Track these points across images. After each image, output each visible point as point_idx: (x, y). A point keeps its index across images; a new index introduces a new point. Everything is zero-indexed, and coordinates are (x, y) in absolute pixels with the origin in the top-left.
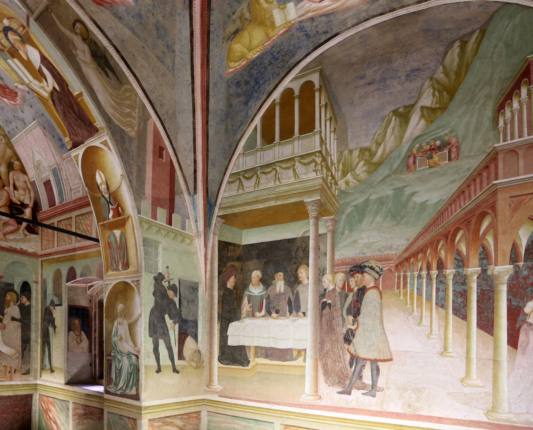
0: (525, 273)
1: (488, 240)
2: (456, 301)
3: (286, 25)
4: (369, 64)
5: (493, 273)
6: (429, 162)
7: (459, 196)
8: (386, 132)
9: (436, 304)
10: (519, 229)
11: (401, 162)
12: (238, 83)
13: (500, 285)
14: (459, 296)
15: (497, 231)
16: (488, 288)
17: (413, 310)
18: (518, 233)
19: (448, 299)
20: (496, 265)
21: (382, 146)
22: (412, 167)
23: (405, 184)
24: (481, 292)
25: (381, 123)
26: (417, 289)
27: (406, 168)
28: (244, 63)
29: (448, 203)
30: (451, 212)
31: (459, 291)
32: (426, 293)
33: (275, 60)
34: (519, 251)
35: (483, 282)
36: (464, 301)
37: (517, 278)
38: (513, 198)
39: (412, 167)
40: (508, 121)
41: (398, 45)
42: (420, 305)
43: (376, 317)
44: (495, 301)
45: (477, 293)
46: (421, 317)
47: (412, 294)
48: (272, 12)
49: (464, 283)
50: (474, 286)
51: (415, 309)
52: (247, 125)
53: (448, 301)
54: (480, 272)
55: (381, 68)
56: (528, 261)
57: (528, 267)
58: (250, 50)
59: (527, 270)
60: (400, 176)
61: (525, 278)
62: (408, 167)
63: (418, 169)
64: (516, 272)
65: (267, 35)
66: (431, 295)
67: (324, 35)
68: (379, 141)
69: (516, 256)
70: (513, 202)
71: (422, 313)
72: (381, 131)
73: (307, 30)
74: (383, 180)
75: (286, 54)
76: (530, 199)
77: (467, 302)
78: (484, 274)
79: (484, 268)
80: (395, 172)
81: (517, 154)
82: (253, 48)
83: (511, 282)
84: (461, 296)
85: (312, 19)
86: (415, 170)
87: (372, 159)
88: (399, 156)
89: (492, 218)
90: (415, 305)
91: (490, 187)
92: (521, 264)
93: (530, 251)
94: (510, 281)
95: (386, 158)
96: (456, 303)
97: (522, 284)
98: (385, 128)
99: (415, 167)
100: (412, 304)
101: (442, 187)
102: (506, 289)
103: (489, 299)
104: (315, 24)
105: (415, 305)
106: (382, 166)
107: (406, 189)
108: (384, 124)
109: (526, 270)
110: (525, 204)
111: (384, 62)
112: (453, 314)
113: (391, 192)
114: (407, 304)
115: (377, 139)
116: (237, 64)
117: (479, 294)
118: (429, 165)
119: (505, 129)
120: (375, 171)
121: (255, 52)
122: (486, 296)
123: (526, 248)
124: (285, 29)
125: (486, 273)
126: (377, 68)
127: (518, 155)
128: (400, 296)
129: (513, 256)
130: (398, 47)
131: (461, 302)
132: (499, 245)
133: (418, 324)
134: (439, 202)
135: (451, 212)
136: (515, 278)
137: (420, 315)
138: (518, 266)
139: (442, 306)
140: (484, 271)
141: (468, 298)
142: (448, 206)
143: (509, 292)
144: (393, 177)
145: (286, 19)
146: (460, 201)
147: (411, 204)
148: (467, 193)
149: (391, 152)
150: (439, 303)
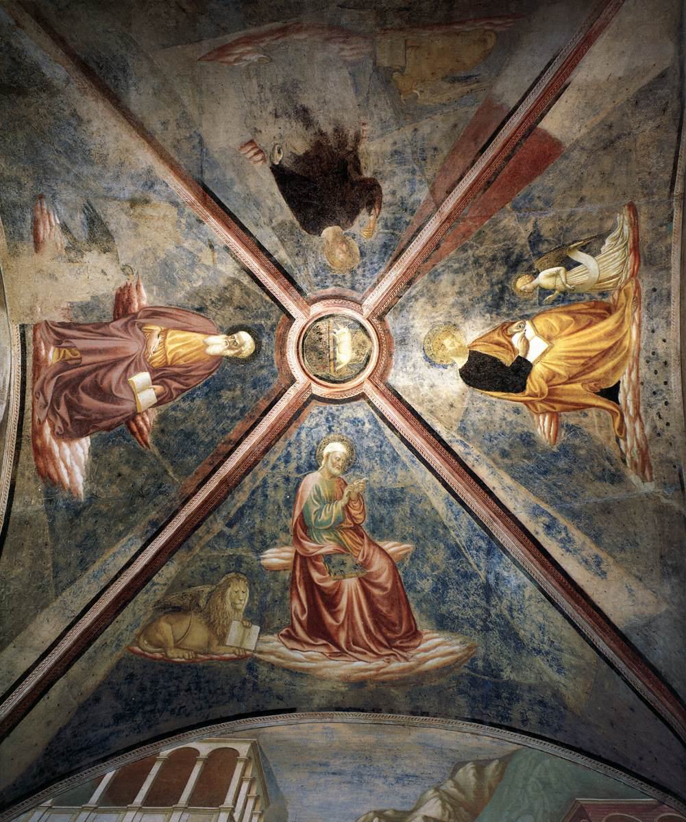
3: (237, 650)
12: (132, 675)
28: (158, 655)
33: (196, 689)
48: (231, 621)
52: (92, 760)
58: (177, 647)
65: (209, 644)
67: (277, 701)
73: (260, 677)
75: (215, 692)
82: (182, 646)
85: (272, 666)
104: (272, 675)
116: (151, 649)
121: (181, 655)
124: (233, 655)
145: (242, 642)
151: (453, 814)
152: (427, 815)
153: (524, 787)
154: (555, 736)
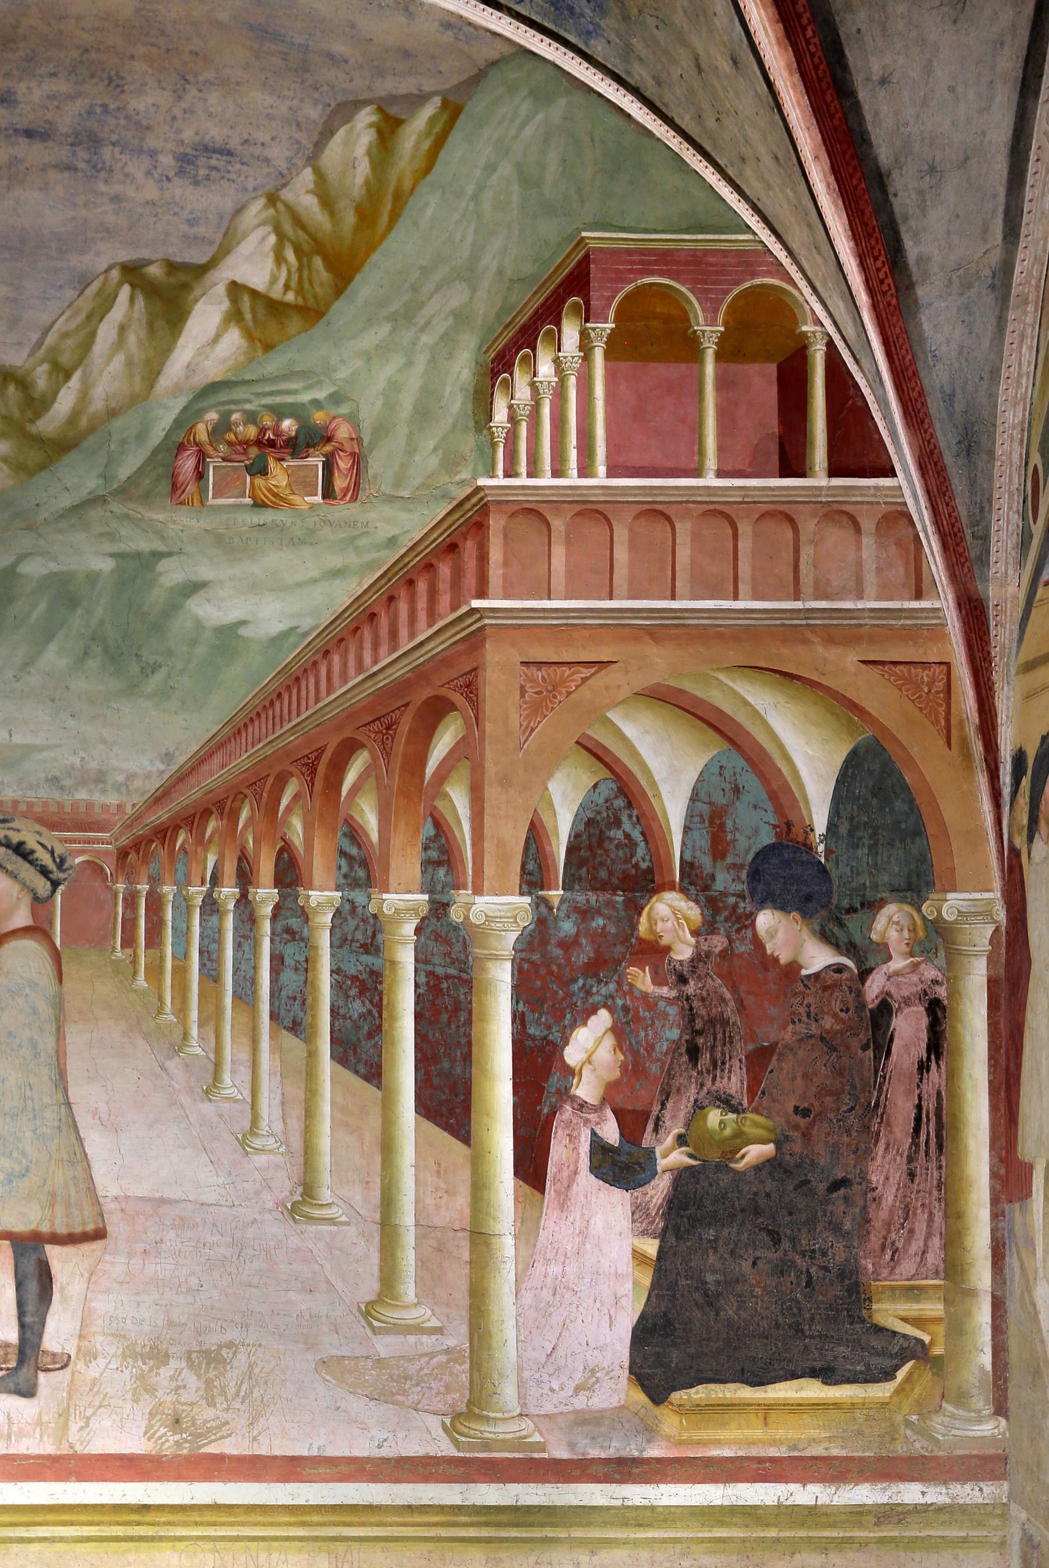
0: (568, 927)
1: (451, 801)
2: (342, 1011)
4: (29, 59)
5: (467, 917)
6: (252, 483)
7: (357, 629)
8: (93, 334)
9: (274, 1016)
10: (550, 775)
11: (149, 461)
13: (490, 965)
14: (353, 992)
15: (483, 773)
16: (452, 971)
17: (186, 1036)
18: (547, 789)
19: (316, 1000)
20: (478, 890)
21: (75, 382)
22: (191, 488)
23: (163, 548)
24: (428, 983)
25: (70, 294)
26: (201, 952)
27: (165, 487)
29: (319, 644)
30: (329, 679)
31: (353, 972)
32: (236, 970)
34: (548, 848)
35: (437, 948)
36: (370, 1012)
37: (544, 942)
38: (533, 669)
39: (191, 488)
40: (523, 413)
41: (153, 40)
42: (211, 1017)
43: (37, 1055)
44: (474, 1018)
45: (417, 986)
46: (218, 1066)
47: (181, 971)
49: (372, 946)
50: (406, 958)
51: (194, 1032)
53: (314, 1007)
54: (424, 910)
55: (79, 95)
56: (577, 887)
57: (577, 909)
59: (574, 917)
60: (143, 511)
61: (568, 945)
62: (174, 487)
63: (211, 501)
64: (541, 922)
66: (254, 982)
68: (65, 359)
69: (540, 866)
70: (531, 680)
71: (218, 1049)
72: (74, 324)
74: (77, 509)
76: (584, 680)
77: (381, 1016)
78: (438, 919)
79: (437, 896)
80: (124, 492)
81: (548, 524)
83: (524, 955)
84: (362, 993)
86: (202, 503)
87: (32, 421)
88: (141, 437)
89: (468, 725)
90: (194, 1014)
91: (461, 619)
92: (555, 894)
93: (582, 853)
94: (521, 951)
95: (91, 430)
96: (344, 1017)
97: (559, 966)
98: (89, 317)
99: (203, 492)
100: (182, 1010)
101: (299, 585)
102: (508, 978)
103: (457, 1009)
105: (194, 1014)
106: (71, 457)
107: (164, 565)
108: (86, 302)
109: (568, 917)
110: (569, 693)
111: (92, 76)
112: (332, 1057)
113: (106, 565)
114: (160, 1010)
115: (54, 350)
117: (421, 991)
118: (253, 496)
119: (512, 437)
120: (42, 467)
122: (447, 999)
123: (569, 841)
125: (446, 915)
126: (61, 86)
127: (550, 530)
128: (135, 973)
129: (531, 866)
130: (152, 45)
131: (362, 1016)
132: (488, 820)
133: (207, 1092)
134: (285, 635)
135: (329, 679)
136: (536, 942)
137: (212, 1056)
138: (545, 901)
139: (295, 1027)
140: (439, 908)
141: (385, 1002)
142: (318, 657)
143: (520, 989)
144: (116, 507)
146: (361, 648)
147: (180, 625)
148: (384, 622)
149: (112, 413)
150: (283, 1013)
151: (295, 277)
152: (239, 280)
153: (475, 198)
154: (586, 44)
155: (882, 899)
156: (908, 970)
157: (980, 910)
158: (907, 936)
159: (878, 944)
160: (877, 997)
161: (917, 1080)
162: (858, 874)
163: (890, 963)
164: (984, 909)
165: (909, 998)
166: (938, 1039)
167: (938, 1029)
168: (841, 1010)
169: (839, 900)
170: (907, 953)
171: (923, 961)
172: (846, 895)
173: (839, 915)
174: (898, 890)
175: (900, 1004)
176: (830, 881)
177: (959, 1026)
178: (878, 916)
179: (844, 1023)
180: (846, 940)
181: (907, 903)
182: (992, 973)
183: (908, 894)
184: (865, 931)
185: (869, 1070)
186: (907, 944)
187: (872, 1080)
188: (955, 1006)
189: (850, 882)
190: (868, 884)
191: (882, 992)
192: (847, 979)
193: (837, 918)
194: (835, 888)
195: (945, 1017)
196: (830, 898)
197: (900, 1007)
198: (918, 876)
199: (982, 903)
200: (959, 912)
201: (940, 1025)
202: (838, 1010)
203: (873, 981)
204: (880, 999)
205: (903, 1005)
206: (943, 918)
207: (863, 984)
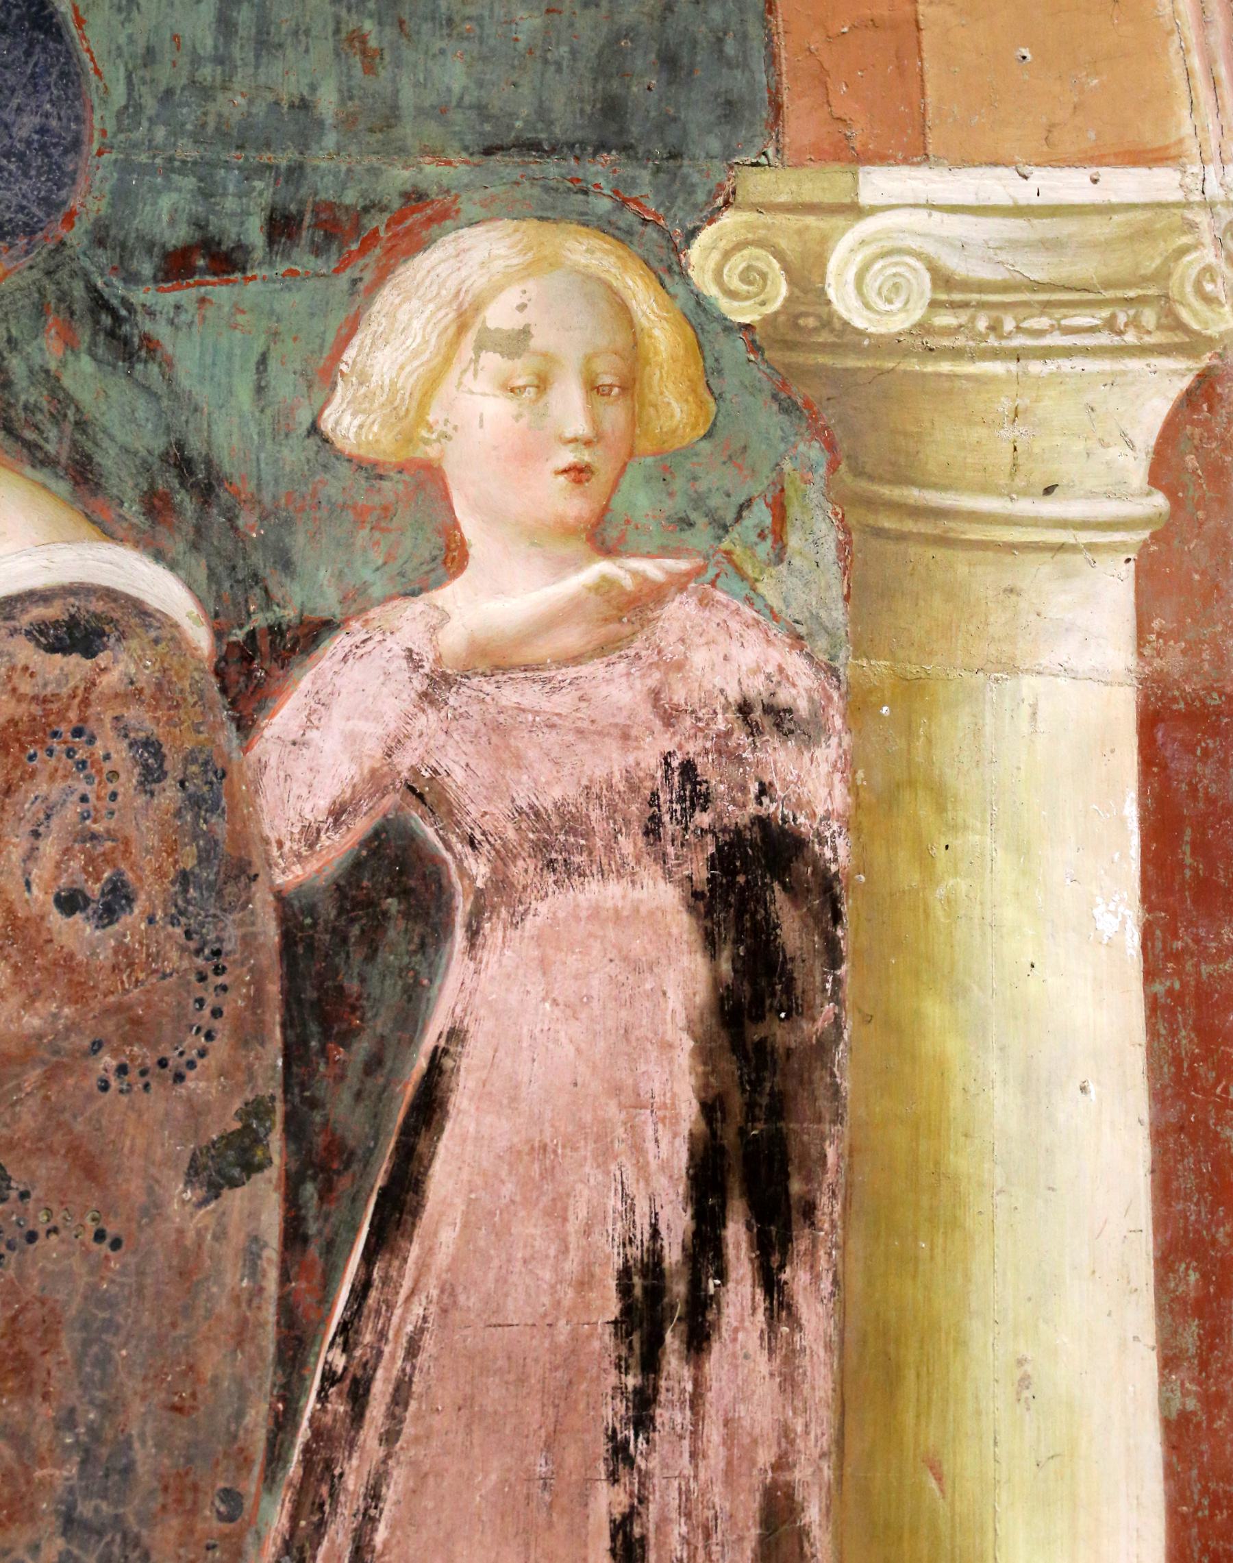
155: (415, 197)
156: (572, 638)
157: (1086, 268)
158: (578, 425)
159: (371, 471)
160: (338, 813)
161: (613, 1412)
162: (265, 44)
163: (452, 595)
164: (1119, 264)
165: (573, 823)
166: (779, 1108)
167: (781, 1034)
168: (70, 902)
169: (122, 195)
170: (566, 530)
171: (680, 583)
172: (172, 167)
173: (115, 290)
174: (531, 147)
175: (503, 857)
176: (71, 77)
177: (934, 1011)
178: (387, 297)
179: (79, 993)
180: (150, 441)
181: (585, 220)
182: (1173, 661)
183: (599, 170)
184: (284, 385)
185: (242, 1334)
186: (579, 473)
187: (258, 1416)
188: (908, 876)
189: (206, 93)
190: (327, 102)
191: (377, 782)
192: (133, 693)
193: (99, 303)
194: (101, 118)
195: (833, 955)
196: (62, 179)
197: (501, 884)
198: (670, 62)
199: (1099, 228)
200: (943, 280)
201: (794, 1009)
202: (41, 898)
203: (321, 704)
204: (361, 826)
205: (522, 870)
206: (828, 321)
207: (245, 726)
